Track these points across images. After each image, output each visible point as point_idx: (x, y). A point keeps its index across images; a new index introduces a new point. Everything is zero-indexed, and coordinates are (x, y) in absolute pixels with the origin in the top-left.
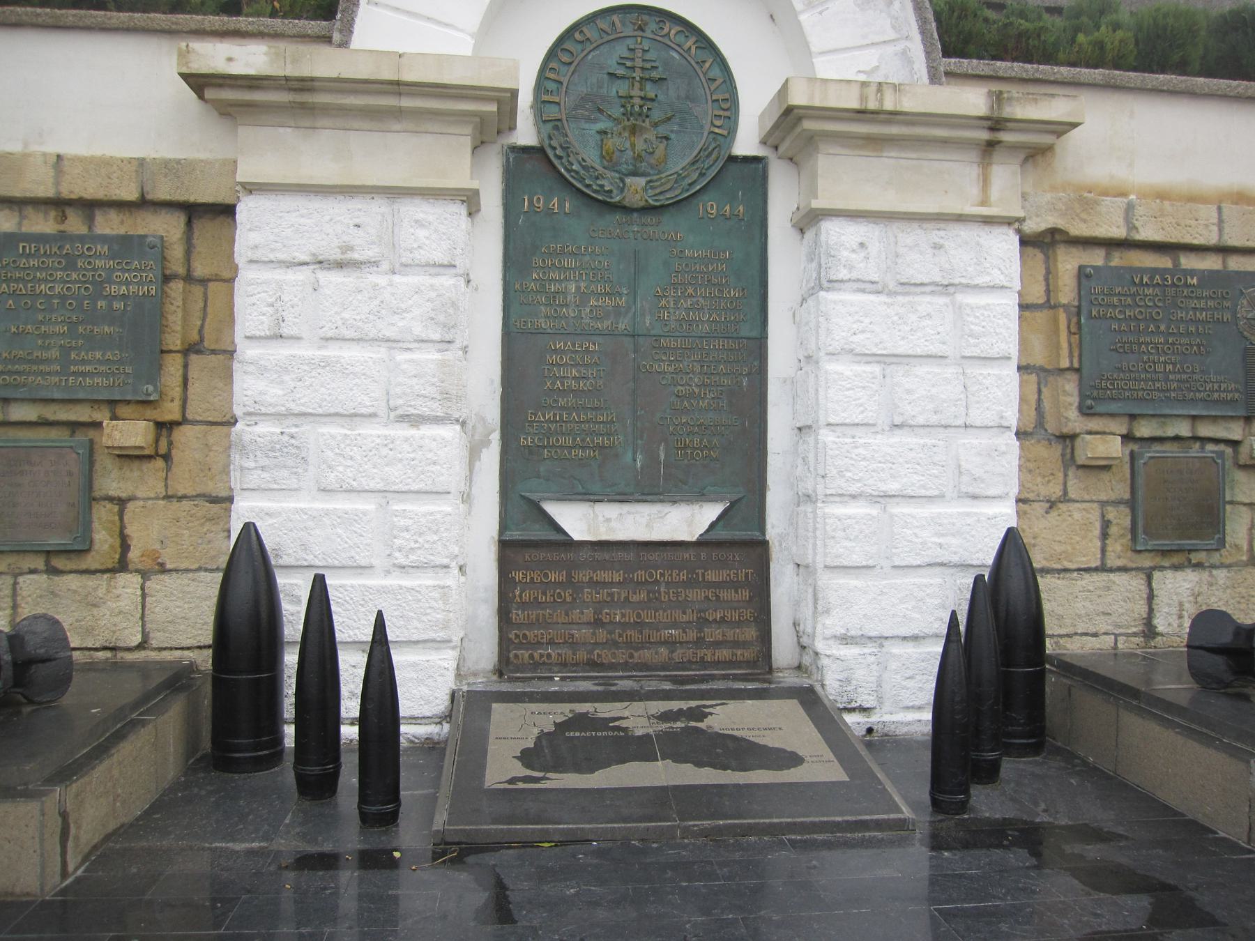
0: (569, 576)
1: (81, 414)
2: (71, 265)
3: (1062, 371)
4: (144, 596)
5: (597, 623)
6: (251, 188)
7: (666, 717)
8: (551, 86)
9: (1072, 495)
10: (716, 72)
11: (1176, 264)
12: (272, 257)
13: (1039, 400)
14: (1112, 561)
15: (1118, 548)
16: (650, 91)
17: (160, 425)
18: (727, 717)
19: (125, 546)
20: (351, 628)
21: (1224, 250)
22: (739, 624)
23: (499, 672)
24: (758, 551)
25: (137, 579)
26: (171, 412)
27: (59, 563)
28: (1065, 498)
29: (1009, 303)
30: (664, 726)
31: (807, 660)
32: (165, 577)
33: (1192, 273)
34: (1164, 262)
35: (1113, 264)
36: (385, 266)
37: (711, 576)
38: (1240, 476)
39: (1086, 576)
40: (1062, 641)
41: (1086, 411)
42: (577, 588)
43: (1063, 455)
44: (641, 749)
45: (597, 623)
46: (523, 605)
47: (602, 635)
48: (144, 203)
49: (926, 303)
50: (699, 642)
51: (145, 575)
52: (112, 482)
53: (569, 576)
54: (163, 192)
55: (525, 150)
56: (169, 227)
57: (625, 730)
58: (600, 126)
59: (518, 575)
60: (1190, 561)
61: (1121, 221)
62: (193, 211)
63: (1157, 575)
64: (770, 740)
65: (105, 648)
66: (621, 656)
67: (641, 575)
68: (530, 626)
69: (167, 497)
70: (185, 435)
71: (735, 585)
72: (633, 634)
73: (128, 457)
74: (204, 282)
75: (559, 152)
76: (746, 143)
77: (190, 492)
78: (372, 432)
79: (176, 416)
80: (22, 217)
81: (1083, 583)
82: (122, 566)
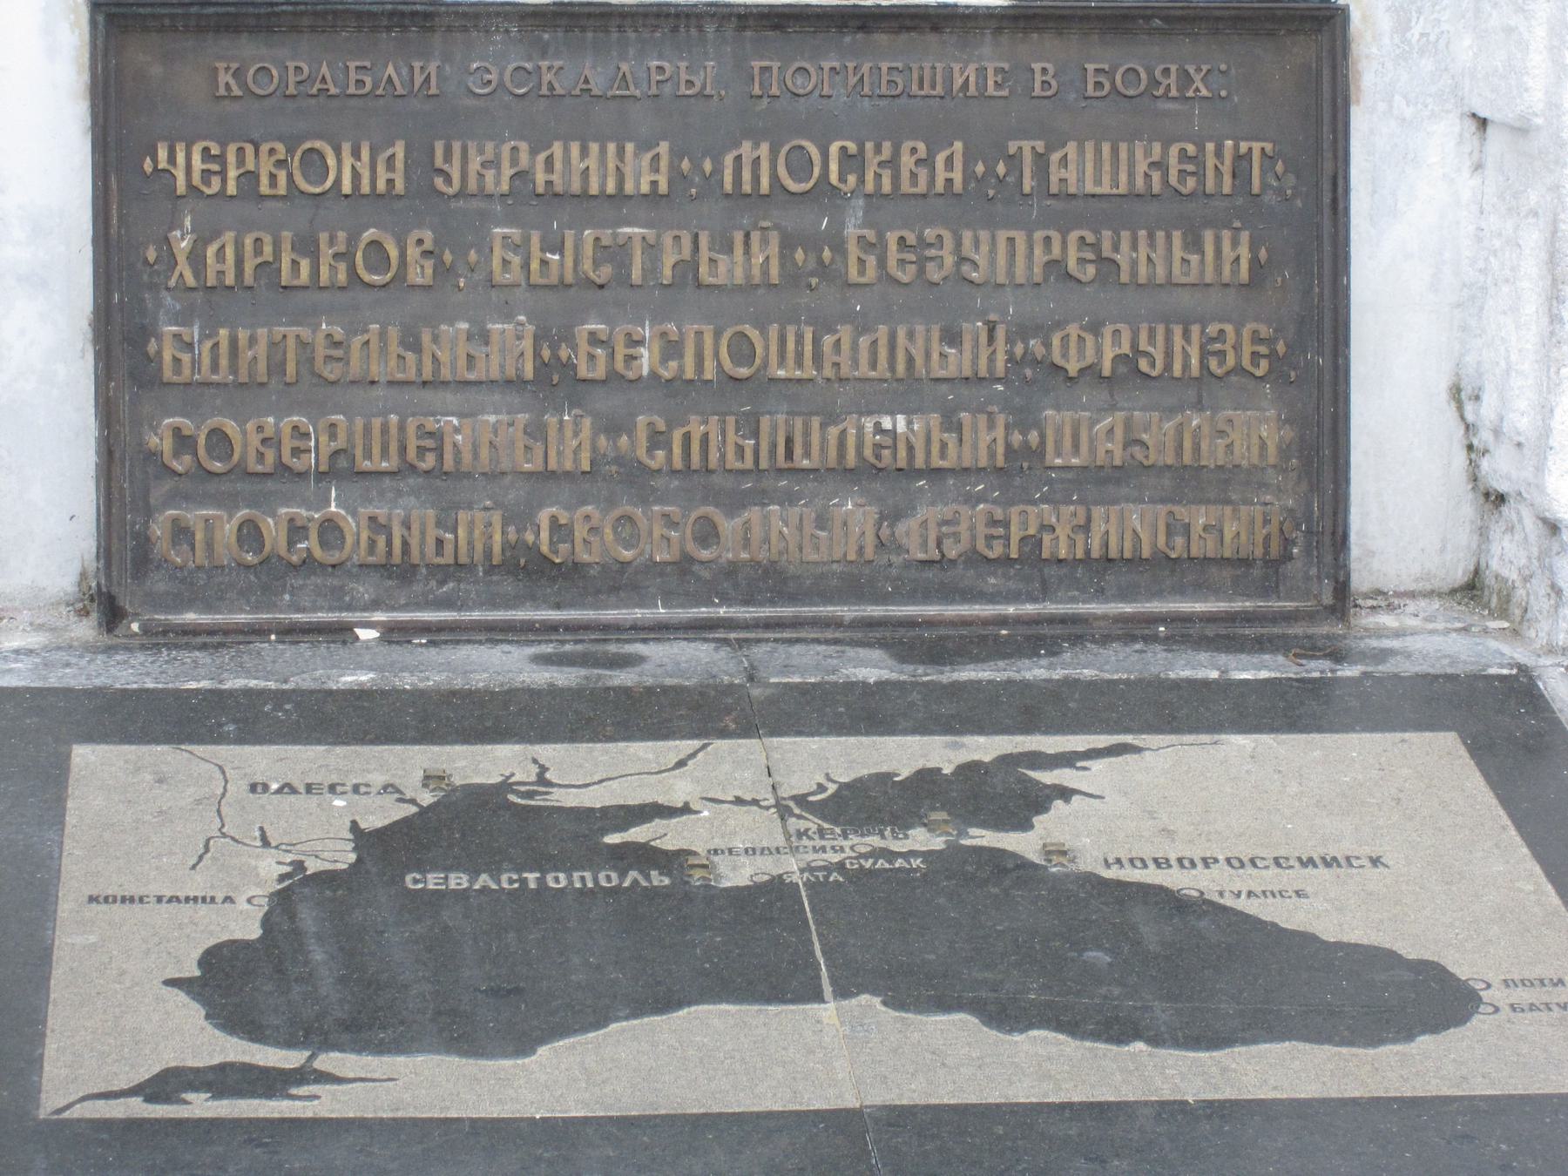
0: (422, 166)
5: (553, 382)
7: (858, 804)
18: (1143, 809)
22: (1201, 388)
23: (106, 606)
30: (853, 847)
31: (1508, 556)
37: (1081, 169)
42: (454, 219)
44: (749, 946)
45: (553, 382)
46: (212, 301)
47: (573, 438)
50: (1018, 471)
53: (422, 166)
57: (673, 861)
59: (186, 164)
64: (1329, 912)
66: (660, 536)
67: (754, 161)
68: (244, 392)
71: (1189, 214)
72: (717, 436)
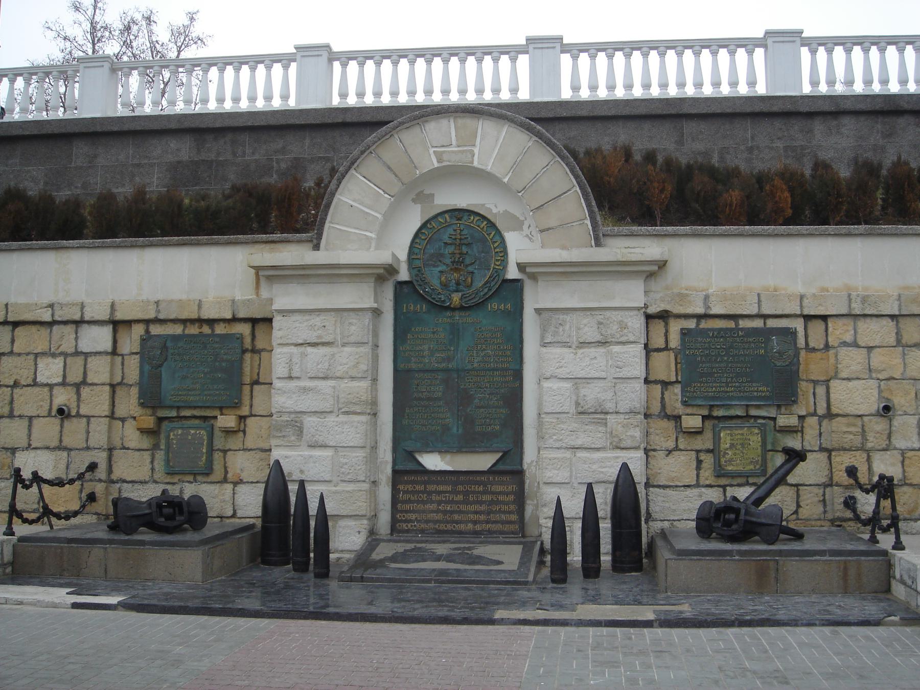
0: (425, 488)
1: (208, 413)
2: (205, 347)
4: (234, 494)
8: (416, 251)
10: (497, 238)
11: (737, 324)
12: (287, 342)
13: (663, 398)
16: (464, 249)
19: (226, 472)
21: (765, 317)
22: (510, 513)
23: (392, 534)
24: (518, 474)
26: (245, 411)
27: (199, 478)
28: (676, 448)
29: (638, 350)
33: (742, 329)
34: (731, 324)
35: (701, 326)
39: (689, 489)
40: (675, 523)
41: (685, 403)
43: (676, 427)
44: (438, 558)
48: (235, 320)
49: (592, 351)
53: (425, 488)
55: (405, 282)
56: (244, 329)
58: (440, 269)
59: (401, 487)
61: (701, 304)
62: (254, 322)
65: (218, 517)
69: (244, 450)
70: (250, 422)
73: (228, 432)
77: (252, 447)
78: (331, 419)
79: (247, 413)
81: (687, 493)
82: (225, 480)
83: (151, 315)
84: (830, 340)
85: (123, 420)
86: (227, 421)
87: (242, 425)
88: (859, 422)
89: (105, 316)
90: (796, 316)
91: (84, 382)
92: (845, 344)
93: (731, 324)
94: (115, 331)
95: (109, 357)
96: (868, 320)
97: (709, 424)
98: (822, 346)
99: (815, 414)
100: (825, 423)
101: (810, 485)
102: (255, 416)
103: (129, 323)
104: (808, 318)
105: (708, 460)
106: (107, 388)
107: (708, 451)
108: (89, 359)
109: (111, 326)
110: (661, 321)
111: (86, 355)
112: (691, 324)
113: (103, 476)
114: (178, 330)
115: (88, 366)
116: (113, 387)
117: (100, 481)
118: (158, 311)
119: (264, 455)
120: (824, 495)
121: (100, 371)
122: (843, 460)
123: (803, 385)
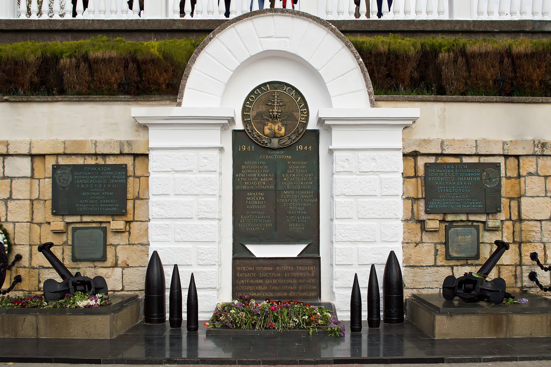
3: (418, 199)
4: (123, 275)
6: (153, 149)
9: (424, 241)
11: (461, 160)
13: (412, 209)
14: (439, 263)
15: (441, 259)
17: (127, 222)
20: (185, 284)
25: (120, 269)
26: (130, 217)
28: (421, 242)
32: (129, 269)
34: (457, 160)
35: (438, 162)
36: (195, 171)
38: (487, 234)
40: (420, 290)
41: (427, 212)
51: (123, 268)
52: (112, 239)
54: (126, 151)
56: (128, 161)
60: (467, 263)
62: (135, 156)
63: (455, 268)
69: (129, 244)
70: (134, 225)
73: (117, 232)
74: (139, 177)
75: (250, 131)
76: (312, 125)
77: (136, 243)
79: (132, 219)
80: (85, 159)
81: (428, 271)
82: (116, 265)
83: (61, 151)
84: (521, 171)
85: (40, 224)
86: (118, 224)
87: (128, 227)
88: (538, 224)
89: (26, 152)
90: (500, 155)
91: (10, 198)
92: (530, 174)
93: (457, 160)
94: (32, 161)
95: (29, 180)
96: (545, 158)
97: (443, 225)
98: (515, 175)
99: (510, 219)
100: (517, 225)
101: (507, 265)
102: (137, 221)
103: (43, 156)
104: (506, 156)
105: (442, 249)
106: (28, 202)
107: (441, 243)
108: (14, 182)
109: (30, 158)
110: (411, 158)
111: (12, 178)
112: (432, 160)
113: (27, 265)
114: (80, 161)
115: (13, 186)
116: (32, 200)
117: (25, 267)
118: (65, 148)
119: (143, 248)
120: (516, 271)
121: (21, 190)
122: (527, 250)
123: (503, 200)
